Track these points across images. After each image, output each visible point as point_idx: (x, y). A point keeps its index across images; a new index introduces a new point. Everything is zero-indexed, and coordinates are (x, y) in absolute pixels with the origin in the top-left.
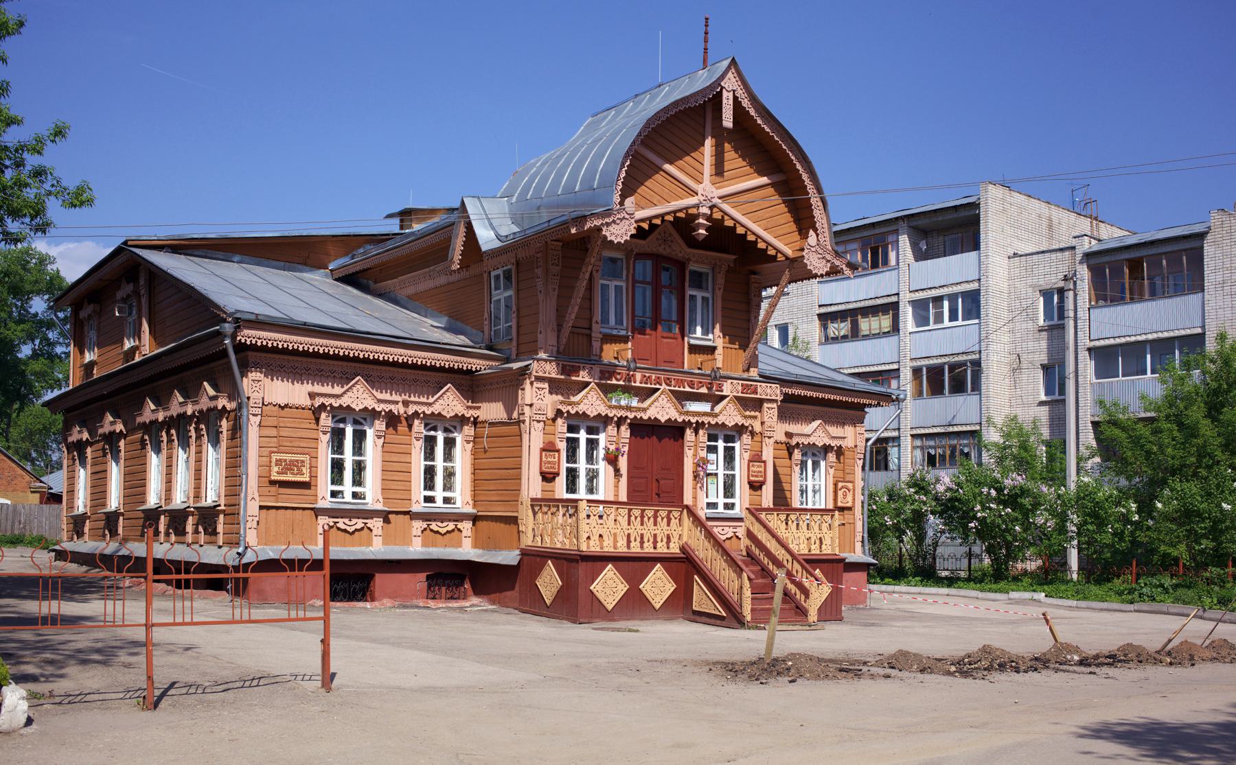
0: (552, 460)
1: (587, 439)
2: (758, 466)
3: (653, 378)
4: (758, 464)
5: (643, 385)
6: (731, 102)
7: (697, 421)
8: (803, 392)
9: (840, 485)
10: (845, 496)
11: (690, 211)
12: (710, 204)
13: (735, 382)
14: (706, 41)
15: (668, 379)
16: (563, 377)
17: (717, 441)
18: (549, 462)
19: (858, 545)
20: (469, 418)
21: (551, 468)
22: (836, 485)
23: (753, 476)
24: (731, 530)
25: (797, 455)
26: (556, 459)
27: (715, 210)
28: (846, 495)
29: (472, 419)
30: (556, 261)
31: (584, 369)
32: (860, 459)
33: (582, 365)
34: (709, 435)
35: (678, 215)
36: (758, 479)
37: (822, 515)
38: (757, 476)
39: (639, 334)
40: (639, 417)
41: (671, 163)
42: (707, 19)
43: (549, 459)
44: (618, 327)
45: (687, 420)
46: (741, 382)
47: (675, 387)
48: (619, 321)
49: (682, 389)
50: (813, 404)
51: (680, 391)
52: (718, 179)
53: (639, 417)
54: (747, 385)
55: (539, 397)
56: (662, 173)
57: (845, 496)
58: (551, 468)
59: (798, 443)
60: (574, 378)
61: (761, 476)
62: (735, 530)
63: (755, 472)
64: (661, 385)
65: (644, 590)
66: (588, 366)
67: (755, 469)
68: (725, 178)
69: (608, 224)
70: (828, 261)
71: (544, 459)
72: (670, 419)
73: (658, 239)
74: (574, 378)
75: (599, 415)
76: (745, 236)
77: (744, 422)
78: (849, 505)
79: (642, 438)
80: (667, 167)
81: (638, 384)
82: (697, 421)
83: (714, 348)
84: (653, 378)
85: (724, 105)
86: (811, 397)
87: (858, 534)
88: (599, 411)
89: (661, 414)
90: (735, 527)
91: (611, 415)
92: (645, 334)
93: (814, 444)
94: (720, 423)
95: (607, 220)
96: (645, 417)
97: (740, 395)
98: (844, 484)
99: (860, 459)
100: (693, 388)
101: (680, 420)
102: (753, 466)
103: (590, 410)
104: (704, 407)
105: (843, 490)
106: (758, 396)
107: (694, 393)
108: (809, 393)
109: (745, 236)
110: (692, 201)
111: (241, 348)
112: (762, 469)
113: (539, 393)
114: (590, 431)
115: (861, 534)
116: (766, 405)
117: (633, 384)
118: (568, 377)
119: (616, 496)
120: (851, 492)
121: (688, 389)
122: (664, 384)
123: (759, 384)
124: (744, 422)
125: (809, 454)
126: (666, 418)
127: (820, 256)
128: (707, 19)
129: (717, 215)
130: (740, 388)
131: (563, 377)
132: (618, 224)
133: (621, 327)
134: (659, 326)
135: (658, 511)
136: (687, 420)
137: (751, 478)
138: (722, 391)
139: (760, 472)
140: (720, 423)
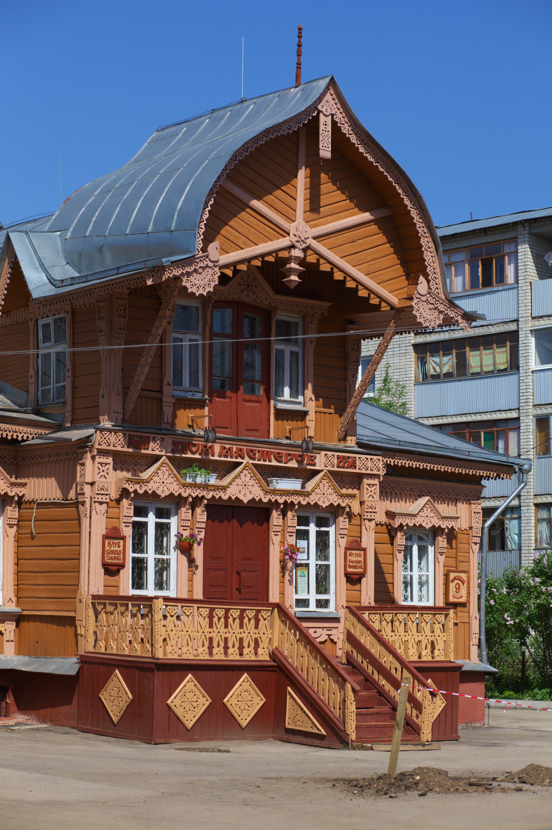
0: (117, 549)
1: (157, 523)
2: (357, 555)
3: (234, 449)
4: (357, 552)
5: (223, 459)
6: (329, 128)
7: (286, 501)
8: (407, 463)
9: (452, 575)
10: (458, 589)
11: (281, 254)
12: (304, 245)
13: (330, 453)
14: (299, 55)
15: (252, 451)
16: (131, 450)
17: (308, 525)
18: (113, 552)
19: (474, 651)
20: (14, 497)
21: (115, 558)
22: (446, 576)
23: (350, 567)
24: (325, 632)
25: (400, 539)
27: (309, 252)
28: (459, 588)
29: (16, 498)
30: (122, 312)
31: (154, 441)
32: (476, 544)
33: (152, 436)
34: (299, 518)
35: (266, 259)
36: (356, 570)
37: (435, 615)
38: (355, 567)
39: (218, 397)
40: (217, 497)
41: (259, 198)
42: (300, 29)
43: (113, 548)
44: (192, 389)
45: (273, 500)
46: (336, 454)
47: (259, 460)
48: (194, 382)
49: (267, 463)
51: (265, 466)
52: (314, 216)
53: (217, 497)
54: (344, 457)
55: (102, 473)
56: (248, 210)
57: (458, 589)
58: (115, 558)
59: (401, 524)
60: (143, 451)
61: (361, 567)
62: (329, 633)
63: (353, 562)
64: (243, 458)
65: (228, 705)
66: (159, 437)
67: (353, 558)
68: (321, 215)
69: (189, 274)
70: (441, 312)
71: (107, 548)
72: (253, 499)
73: (240, 284)
74: (143, 451)
75: (172, 494)
77: (340, 501)
78: (463, 600)
79: (221, 521)
80: (255, 203)
81: (216, 458)
82: (286, 501)
84: (234, 449)
85: (321, 132)
86: (417, 469)
87: (474, 636)
88: (171, 490)
89: (243, 492)
90: (329, 629)
91: (185, 495)
92: (224, 397)
93: (420, 525)
94: (312, 503)
95: (188, 269)
96: (225, 497)
97: (336, 469)
99: (476, 544)
100: (280, 462)
101: (265, 500)
102: (350, 554)
103: (161, 489)
104: (294, 484)
105: (456, 582)
106: (357, 471)
107: (281, 467)
108: (415, 464)
109: (344, 282)
110: (284, 242)
112: (361, 559)
113: (102, 469)
114: (160, 514)
115: (478, 636)
116: (365, 481)
117: (211, 458)
118: (137, 451)
119: (191, 591)
120: (465, 585)
121: (274, 463)
122: (246, 457)
123: (357, 456)
124: (340, 501)
125: (415, 538)
126: (250, 497)
127: (432, 306)
128: (300, 29)
129: (312, 259)
130: (336, 461)
131: (131, 450)
132: (200, 274)
133: (196, 389)
134: (242, 388)
135: (245, 610)
136: (273, 500)
137: (349, 570)
138: (314, 465)
139: (359, 562)
140: (312, 503)
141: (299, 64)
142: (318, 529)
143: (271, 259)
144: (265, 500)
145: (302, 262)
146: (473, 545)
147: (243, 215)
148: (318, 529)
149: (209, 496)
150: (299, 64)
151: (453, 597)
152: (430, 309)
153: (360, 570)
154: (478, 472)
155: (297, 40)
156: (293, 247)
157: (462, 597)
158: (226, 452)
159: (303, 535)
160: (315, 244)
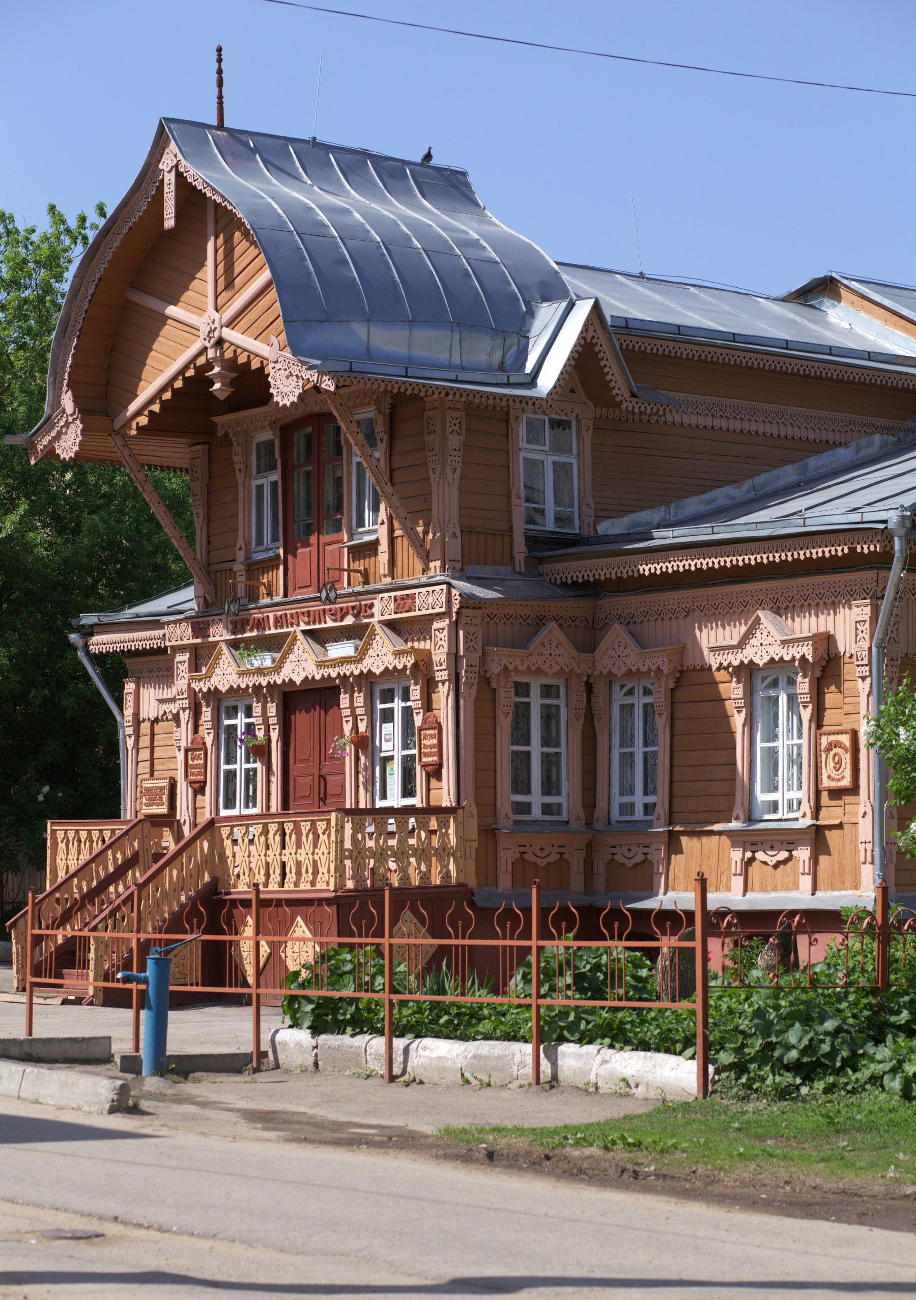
5: (279, 631)
6: (173, 187)
8: (705, 563)
10: (838, 765)
12: (213, 340)
13: (386, 595)
15: (303, 613)
16: (199, 641)
17: (393, 701)
18: (195, 767)
26: (202, 762)
27: (226, 345)
32: (863, 678)
33: (210, 619)
37: (247, 826)
42: (219, 50)
43: (196, 762)
45: (326, 675)
46: (393, 594)
47: (314, 623)
49: (323, 626)
50: (706, 585)
54: (403, 598)
66: (217, 618)
68: (237, 288)
71: (190, 762)
72: (307, 678)
76: (175, 392)
78: (846, 782)
80: (171, 310)
81: (273, 631)
83: (376, 542)
86: (759, 565)
87: (861, 847)
97: (394, 616)
98: (832, 738)
101: (318, 677)
105: (835, 751)
111: (100, 659)
112: (435, 741)
117: (268, 632)
118: (205, 640)
121: (330, 624)
123: (416, 591)
126: (302, 677)
128: (219, 50)
131: (199, 641)
133: (277, 544)
136: (326, 675)
137: (424, 759)
141: (220, 97)
142: (404, 704)
143: (190, 373)
144: (318, 677)
145: (222, 360)
146: (860, 680)
147: (166, 330)
148: (404, 704)
149: (264, 683)
150: (220, 97)
151: (829, 777)
152: (287, 377)
153: (435, 758)
154: (865, 547)
155: (216, 65)
156: (205, 350)
157: (843, 777)
158: (279, 622)
159: (388, 716)
160: (227, 333)
